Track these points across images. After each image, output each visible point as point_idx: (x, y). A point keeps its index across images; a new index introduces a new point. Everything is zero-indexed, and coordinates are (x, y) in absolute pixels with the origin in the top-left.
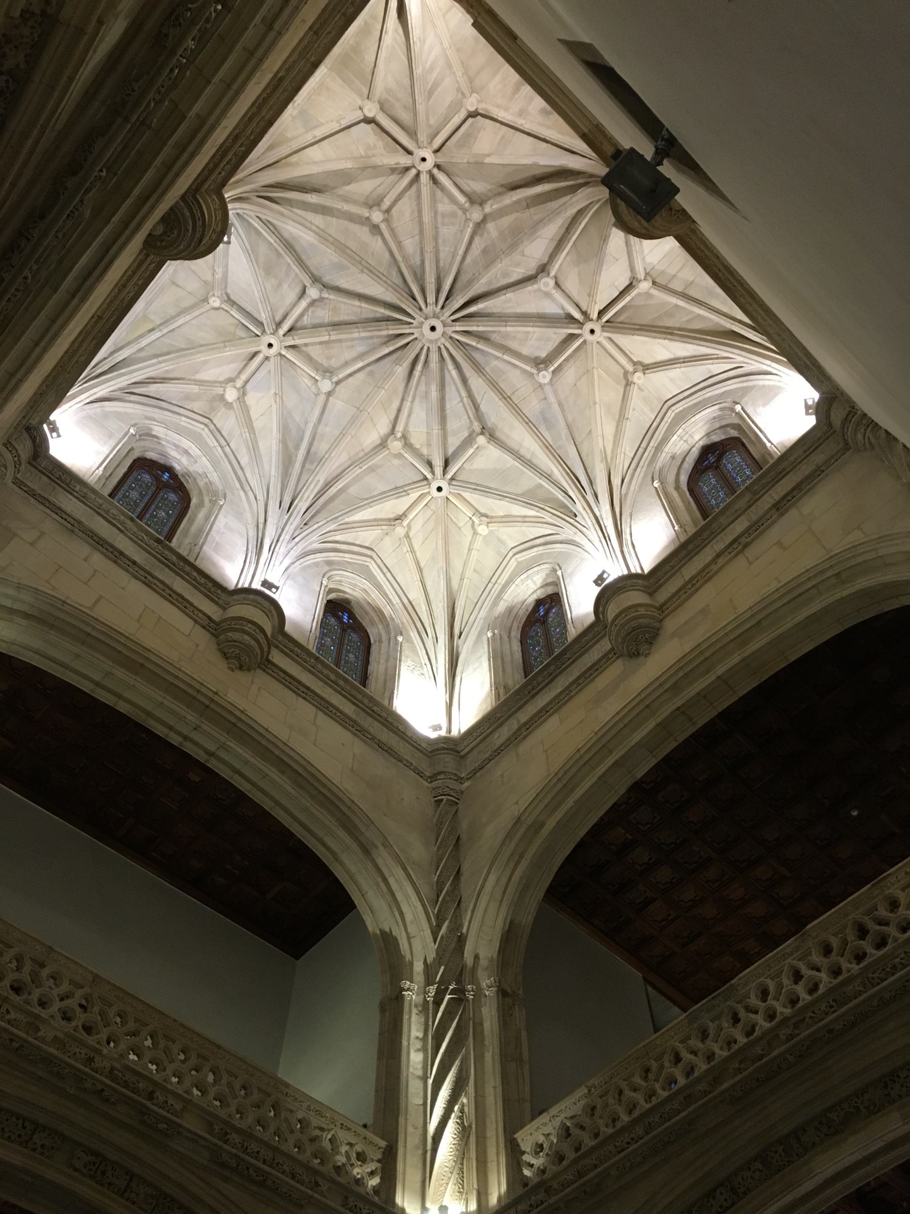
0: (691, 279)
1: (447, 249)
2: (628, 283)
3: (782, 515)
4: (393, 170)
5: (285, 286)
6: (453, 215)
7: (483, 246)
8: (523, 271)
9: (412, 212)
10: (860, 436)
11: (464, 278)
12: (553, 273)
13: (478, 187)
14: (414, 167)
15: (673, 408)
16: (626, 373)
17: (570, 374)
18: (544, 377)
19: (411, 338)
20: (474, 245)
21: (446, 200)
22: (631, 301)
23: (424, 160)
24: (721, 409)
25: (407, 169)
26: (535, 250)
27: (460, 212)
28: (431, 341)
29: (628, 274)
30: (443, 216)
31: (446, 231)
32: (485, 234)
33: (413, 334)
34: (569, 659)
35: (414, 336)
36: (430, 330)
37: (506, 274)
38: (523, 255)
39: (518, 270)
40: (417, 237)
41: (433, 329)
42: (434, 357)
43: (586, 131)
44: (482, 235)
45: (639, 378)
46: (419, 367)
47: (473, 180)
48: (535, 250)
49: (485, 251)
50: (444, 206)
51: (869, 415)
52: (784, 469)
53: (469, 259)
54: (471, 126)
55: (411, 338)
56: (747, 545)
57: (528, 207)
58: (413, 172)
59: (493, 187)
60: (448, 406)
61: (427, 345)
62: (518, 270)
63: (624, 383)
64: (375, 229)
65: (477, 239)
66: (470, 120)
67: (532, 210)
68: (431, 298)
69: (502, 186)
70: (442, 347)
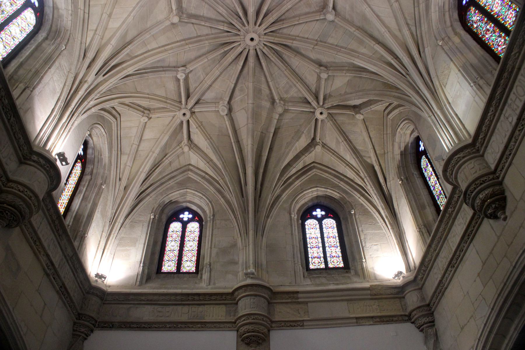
0: (172, 165)
1: (276, 73)
2: (192, 137)
3: (57, 292)
4: (330, 96)
5: (348, 8)
6: (287, 92)
7: (263, 92)
8: (236, 99)
9: (306, 78)
10: (83, 330)
11: (258, 69)
12: (225, 117)
13: (288, 117)
14: (322, 106)
15: (116, 123)
16: (149, 110)
17: (171, 86)
18: (181, 76)
19: (258, 24)
20: (267, 88)
21: (295, 95)
22: (183, 133)
23: (321, 113)
24: (105, 165)
25: (325, 99)
26: (242, 118)
27: (285, 96)
28: (247, 32)
29: (196, 142)
30: (291, 87)
31: (283, 82)
32: (266, 98)
33: (259, 26)
34: (9, 120)
35: (257, 26)
36: (252, 37)
37: (242, 90)
38: (243, 109)
39: (239, 97)
40: (294, 67)
41: (252, 39)
42: (238, 25)
43: (300, 295)
44: (267, 96)
45: (144, 120)
46: (241, 14)
47: (292, 119)
48: (242, 118)
49: (260, 90)
50: (293, 93)
51: (92, 334)
52: (77, 272)
53: (263, 79)
54: (311, 136)
55: (258, 24)
56: (48, 275)
57: (262, 132)
58: (321, 104)
59: (282, 124)
60: (207, 6)
61: (247, 27)
62: (239, 97)
63: (146, 107)
64: (320, 64)
65: (267, 91)
66: (312, 137)
67: (259, 133)
68: (266, 50)
69: (279, 128)
70: (239, 33)
